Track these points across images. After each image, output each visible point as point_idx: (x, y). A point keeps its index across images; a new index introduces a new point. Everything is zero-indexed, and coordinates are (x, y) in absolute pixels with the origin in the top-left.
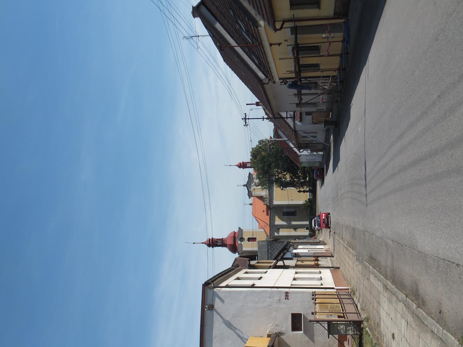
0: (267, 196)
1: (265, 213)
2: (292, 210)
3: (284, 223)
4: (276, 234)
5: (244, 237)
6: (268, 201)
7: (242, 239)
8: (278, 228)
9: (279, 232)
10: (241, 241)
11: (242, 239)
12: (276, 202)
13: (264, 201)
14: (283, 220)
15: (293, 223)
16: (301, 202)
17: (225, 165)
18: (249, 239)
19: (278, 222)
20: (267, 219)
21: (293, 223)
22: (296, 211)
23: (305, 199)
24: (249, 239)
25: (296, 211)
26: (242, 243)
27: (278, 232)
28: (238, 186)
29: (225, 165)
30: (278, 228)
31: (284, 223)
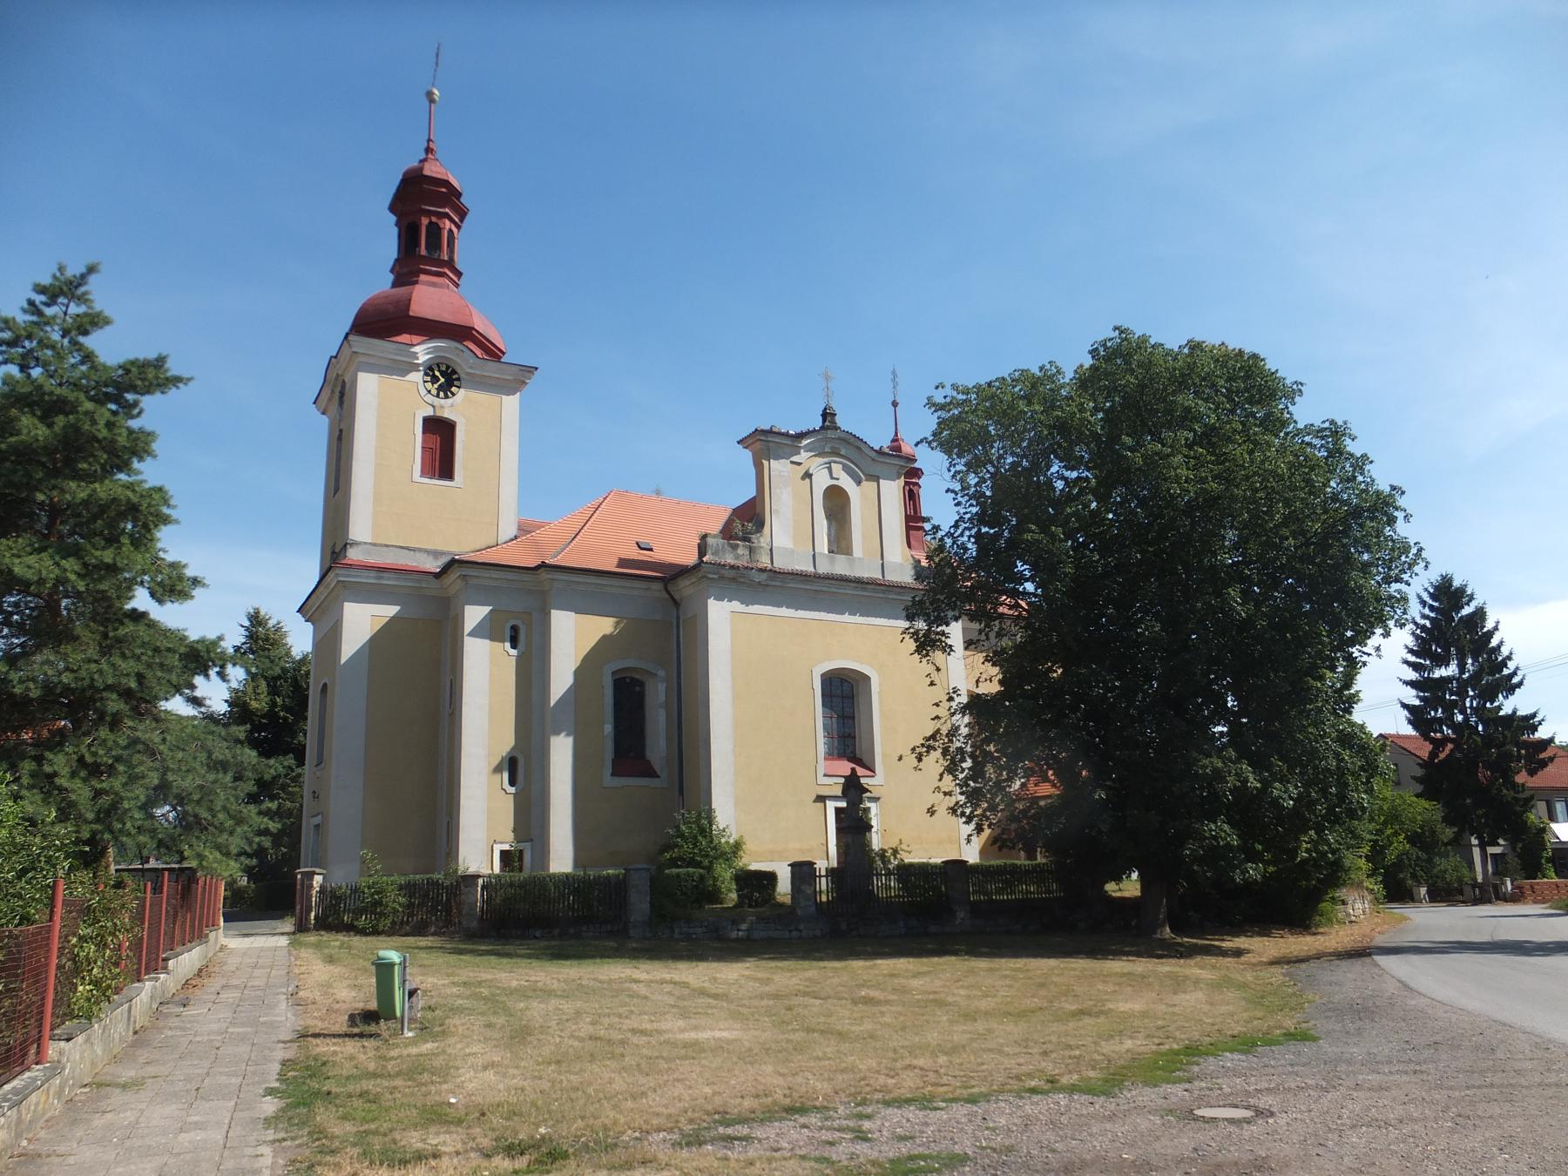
0: (764, 561)
1: (635, 554)
2: (657, 746)
3: (561, 679)
4: (474, 614)
5: (461, 394)
6: (729, 559)
7: (446, 378)
8: (524, 636)
9: (494, 636)
10: (429, 370)
11: (446, 378)
12: (724, 621)
13: (727, 532)
14: (583, 673)
15: (561, 751)
16: (727, 811)
17: (894, 372)
18: (440, 433)
19: (573, 636)
20: (603, 549)
21: (561, 751)
22: (649, 772)
23: (750, 846)
24: (440, 433)
25: (649, 772)
26: (417, 377)
27: (487, 630)
28: (827, 378)
29: (894, 372)
30: (524, 636)
31: (561, 679)
